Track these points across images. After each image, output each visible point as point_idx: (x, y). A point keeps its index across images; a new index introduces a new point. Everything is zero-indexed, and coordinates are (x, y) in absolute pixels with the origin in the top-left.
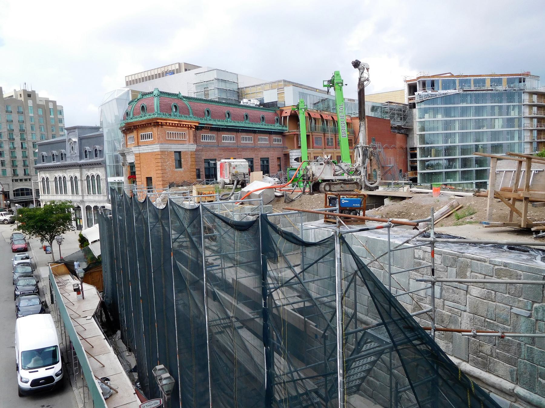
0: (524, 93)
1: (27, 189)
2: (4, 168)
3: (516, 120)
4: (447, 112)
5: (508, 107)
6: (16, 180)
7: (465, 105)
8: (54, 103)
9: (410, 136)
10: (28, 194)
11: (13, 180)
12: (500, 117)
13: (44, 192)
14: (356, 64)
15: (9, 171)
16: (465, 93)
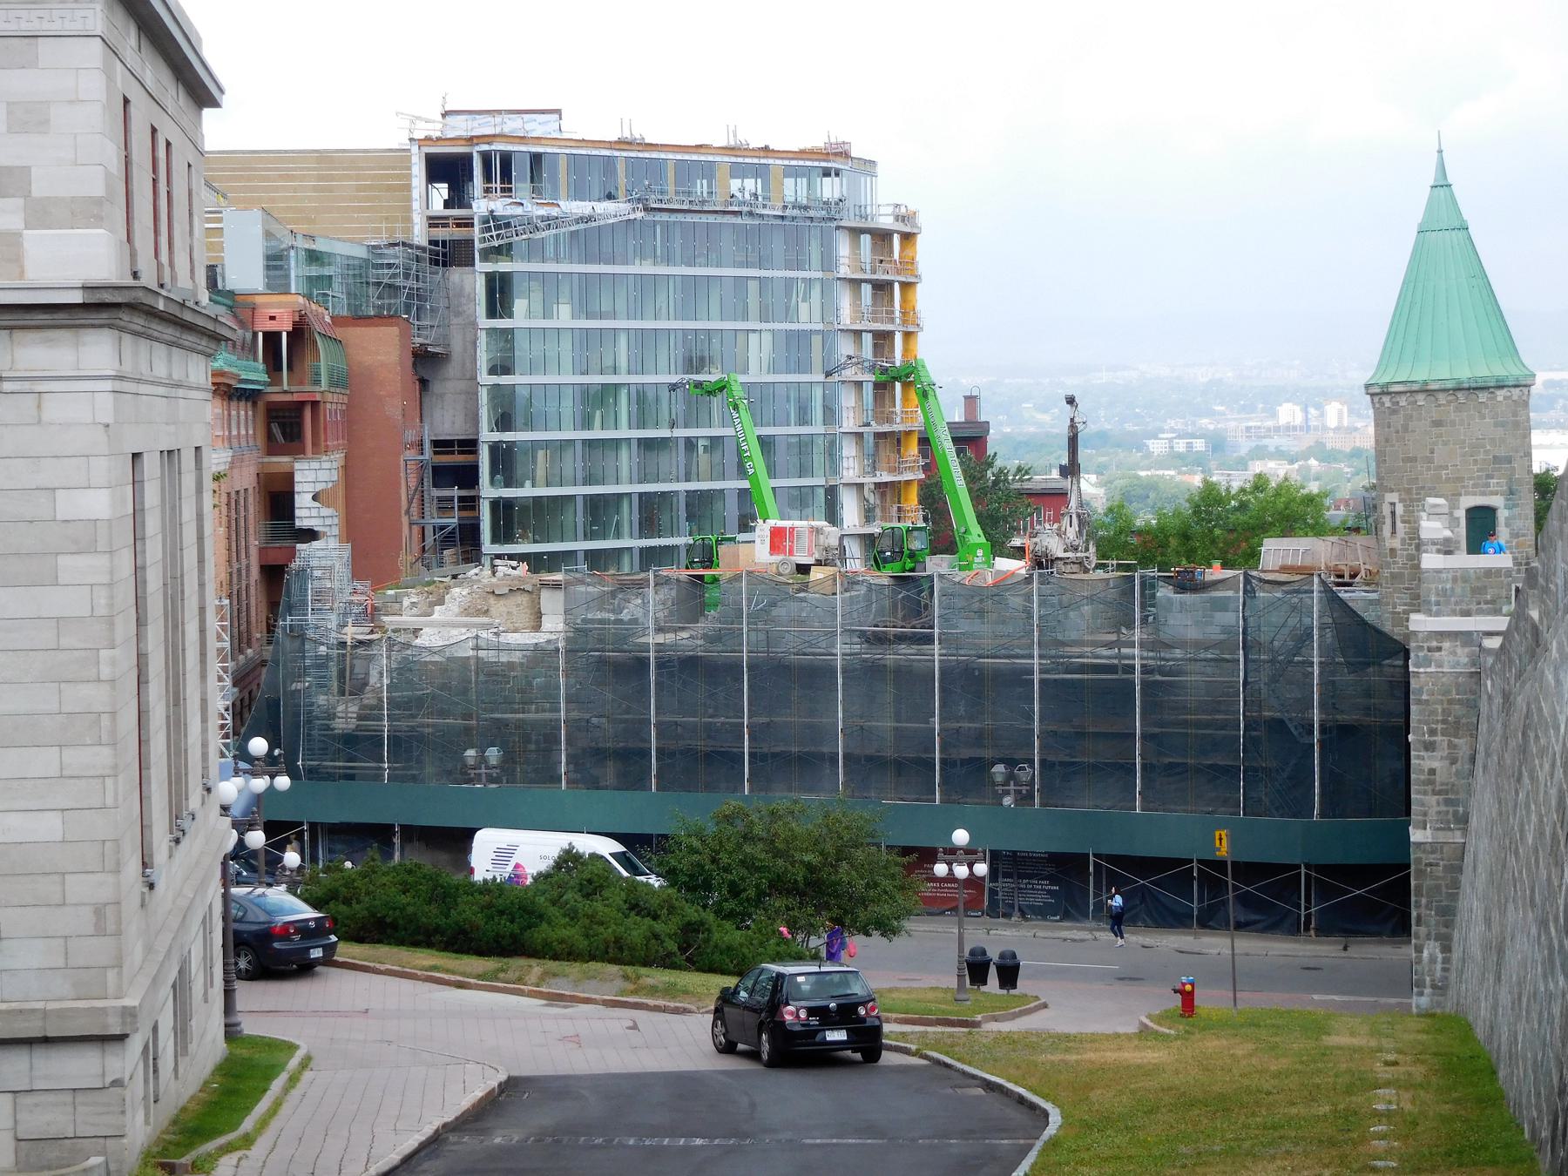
0: (838, 228)
3: (817, 341)
4: (587, 294)
5: (789, 283)
7: (647, 268)
9: (436, 387)
12: (764, 326)
14: (1071, 401)
16: (649, 217)
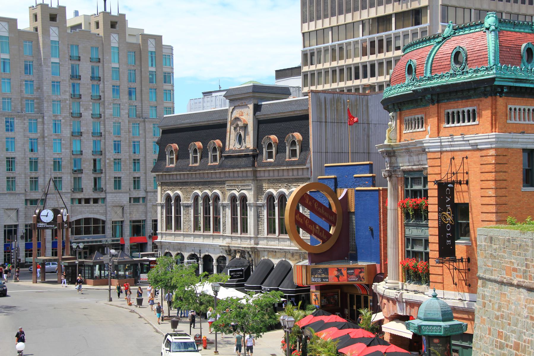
1: (96, 221)
2: (11, 175)
6: (80, 201)
8: (158, 39)
10: (96, 231)
11: (73, 200)
13: (168, 227)
15: (67, 180)
